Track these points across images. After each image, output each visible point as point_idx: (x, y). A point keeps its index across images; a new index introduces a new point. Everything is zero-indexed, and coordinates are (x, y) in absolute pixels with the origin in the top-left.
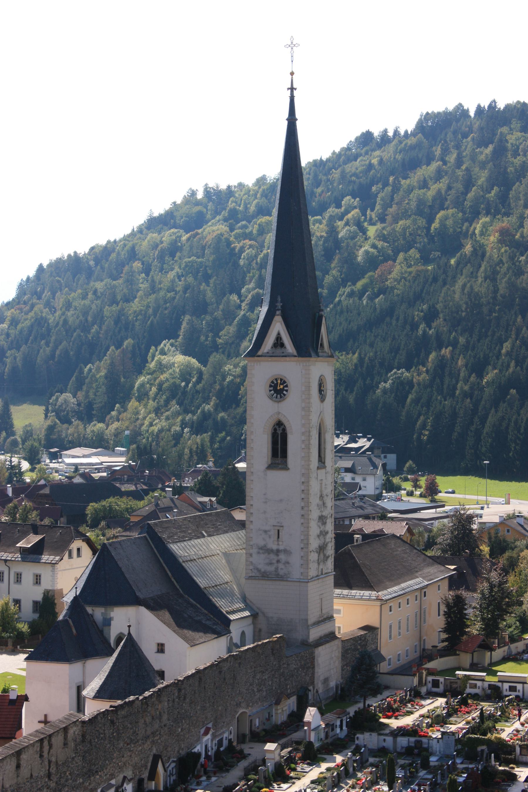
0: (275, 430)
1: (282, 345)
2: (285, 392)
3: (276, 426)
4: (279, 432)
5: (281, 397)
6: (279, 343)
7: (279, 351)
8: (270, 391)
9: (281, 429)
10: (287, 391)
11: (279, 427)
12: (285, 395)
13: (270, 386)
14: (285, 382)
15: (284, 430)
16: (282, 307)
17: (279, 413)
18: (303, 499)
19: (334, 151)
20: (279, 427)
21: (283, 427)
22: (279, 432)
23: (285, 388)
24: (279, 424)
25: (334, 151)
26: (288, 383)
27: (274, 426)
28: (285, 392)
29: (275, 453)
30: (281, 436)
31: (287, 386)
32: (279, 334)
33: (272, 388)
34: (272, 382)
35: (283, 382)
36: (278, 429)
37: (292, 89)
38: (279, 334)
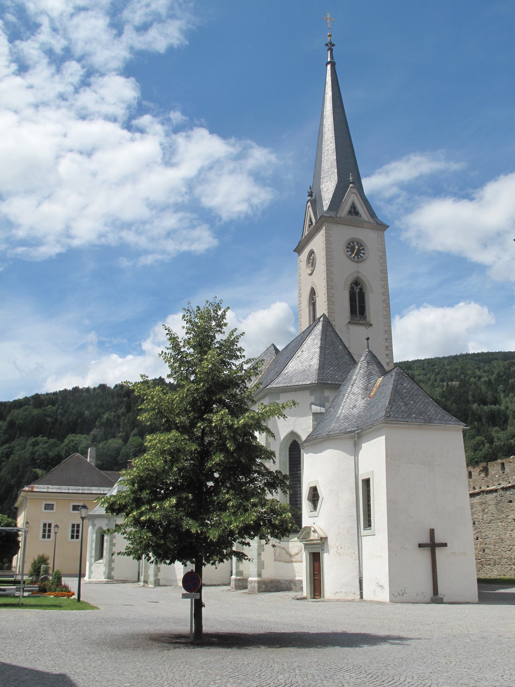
1: (357, 213)
3: (353, 285)
4: (357, 290)
6: (354, 211)
9: (359, 287)
11: (357, 286)
13: (348, 247)
15: (361, 289)
17: (359, 272)
18: (387, 355)
20: (357, 286)
22: (357, 290)
27: (351, 285)
29: (353, 311)
30: (358, 294)
31: (363, 249)
33: (349, 250)
34: (349, 244)
35: (361, 244)
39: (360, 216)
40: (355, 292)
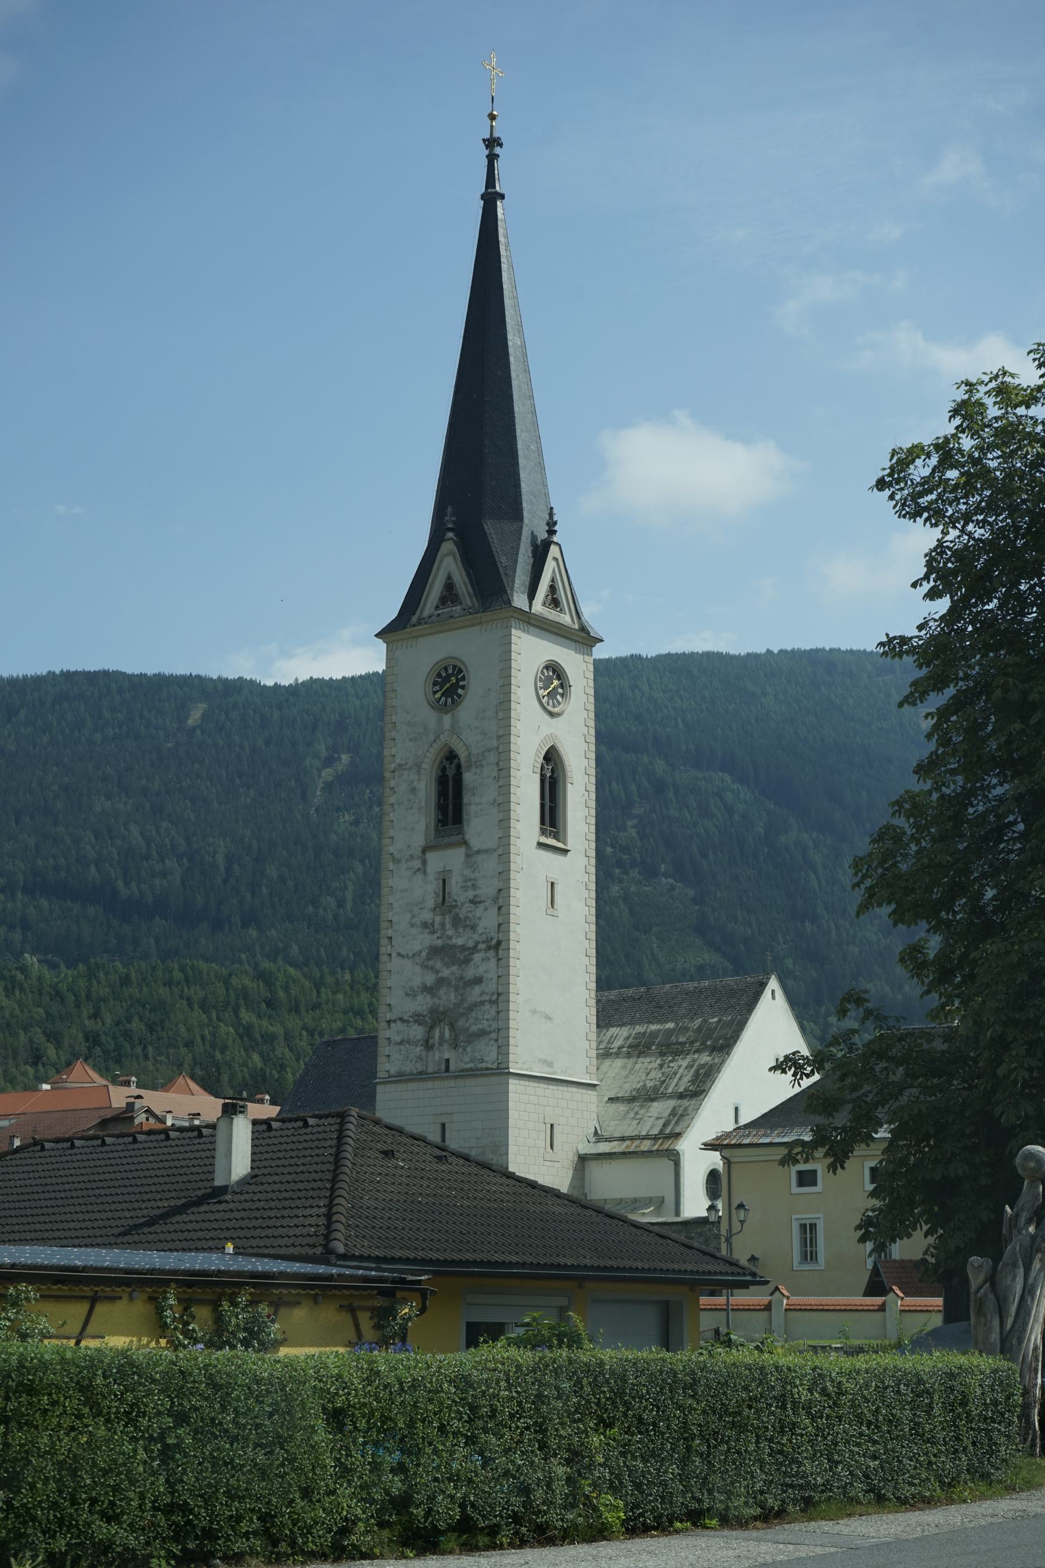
0: (444, 769)
2: (460, 691)
4: (451, 772)
5: (453, 702)
6: (449, 595)
8: (435, 693)
10: (463, 687)
11: (451, 763)
12: (459, 696)
14: (460, 671)
19: (484, 140)
21: (455, 761)
22: (451, 772)
23: (461, 683)
24: (451, 756)
25: (484, 140)
28: (460, 691)
32: (449, 577)
34: (439, 675)
37: (492, 143)
38: (449, 577)
40: (448, 776)
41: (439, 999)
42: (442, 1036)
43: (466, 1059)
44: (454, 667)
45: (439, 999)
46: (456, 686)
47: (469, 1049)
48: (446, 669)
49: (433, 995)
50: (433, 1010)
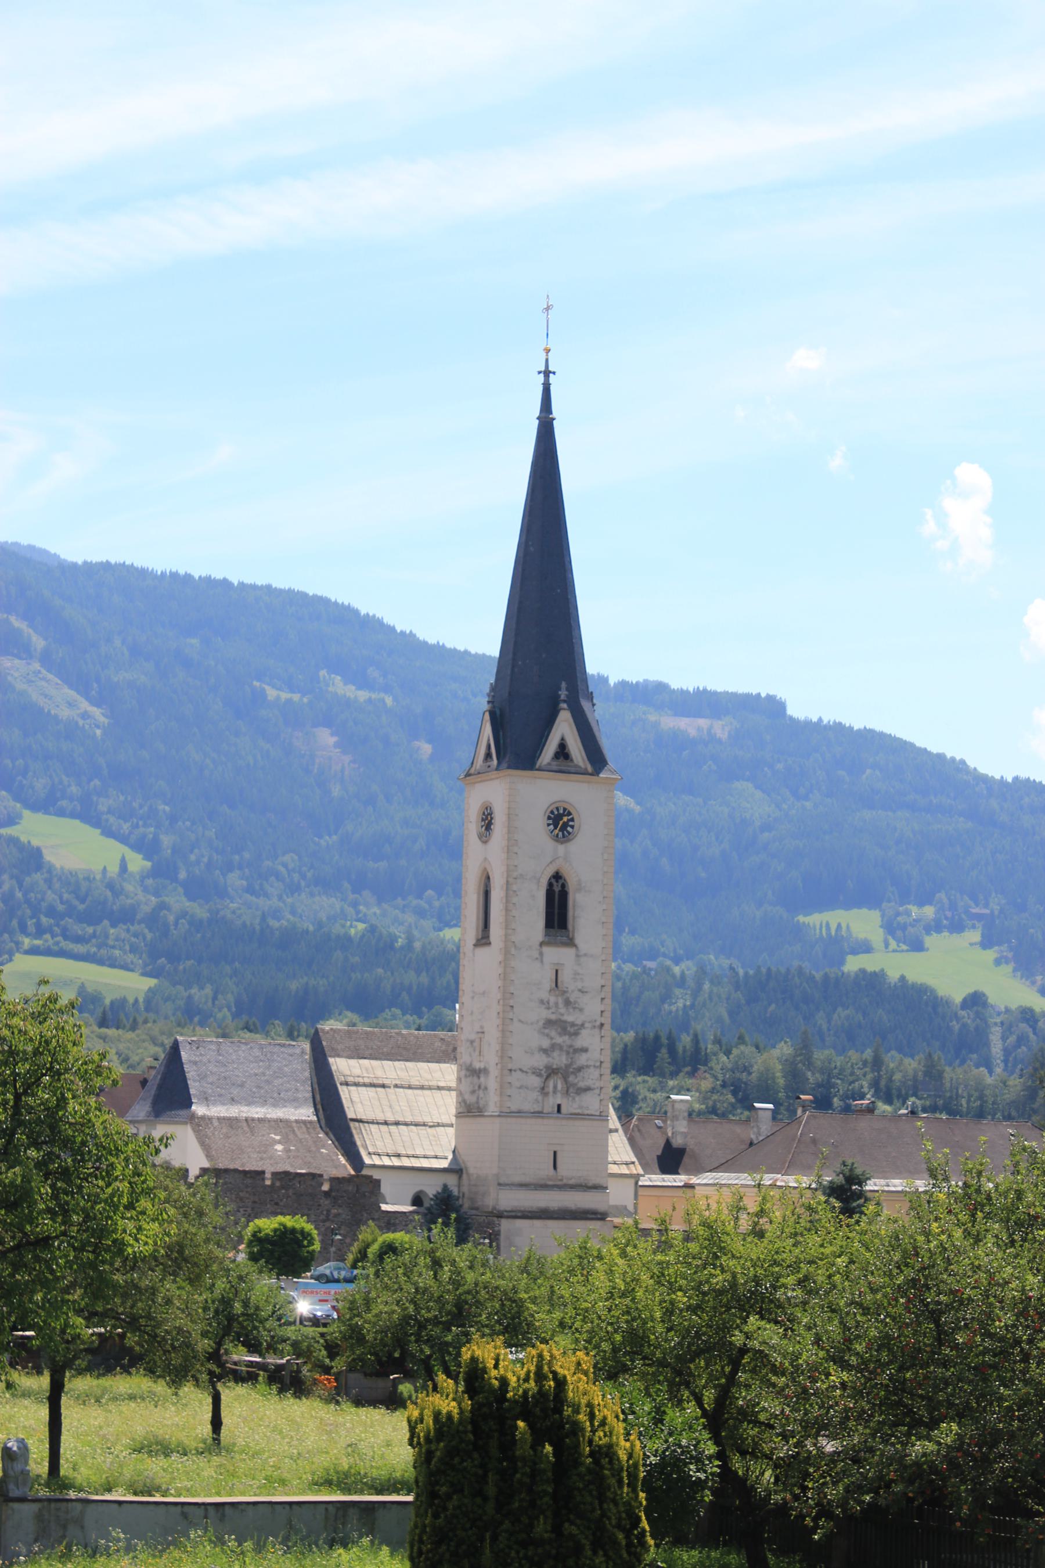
0: (550, 885)
2: (569, 829)
3: (553, 881)
4: (557, 888)
6: (562, 752)
7: (561, 763)
15: (563, 886)
16: (567, 696)
21: (561, 882)
22: (557, 888)
23: (571, 823)
24: (557, 876)
26: (575, 815)
30: (559, 895)
31: (572, 820)
32: (563, 739)
34: (552, 812)
36: (555, 884)
38: (563, 739)
39: (572, 760)
40: (554, 891)
41: (553, 1058)
42: (555, 1087)
43: (575, 1105)
44: (565, 809)
45: (553, 1058)
46: (565, 825)
47: (577, 1099)
48: (557, 809)
49: (548, 1055)
50: (547, 1067)
